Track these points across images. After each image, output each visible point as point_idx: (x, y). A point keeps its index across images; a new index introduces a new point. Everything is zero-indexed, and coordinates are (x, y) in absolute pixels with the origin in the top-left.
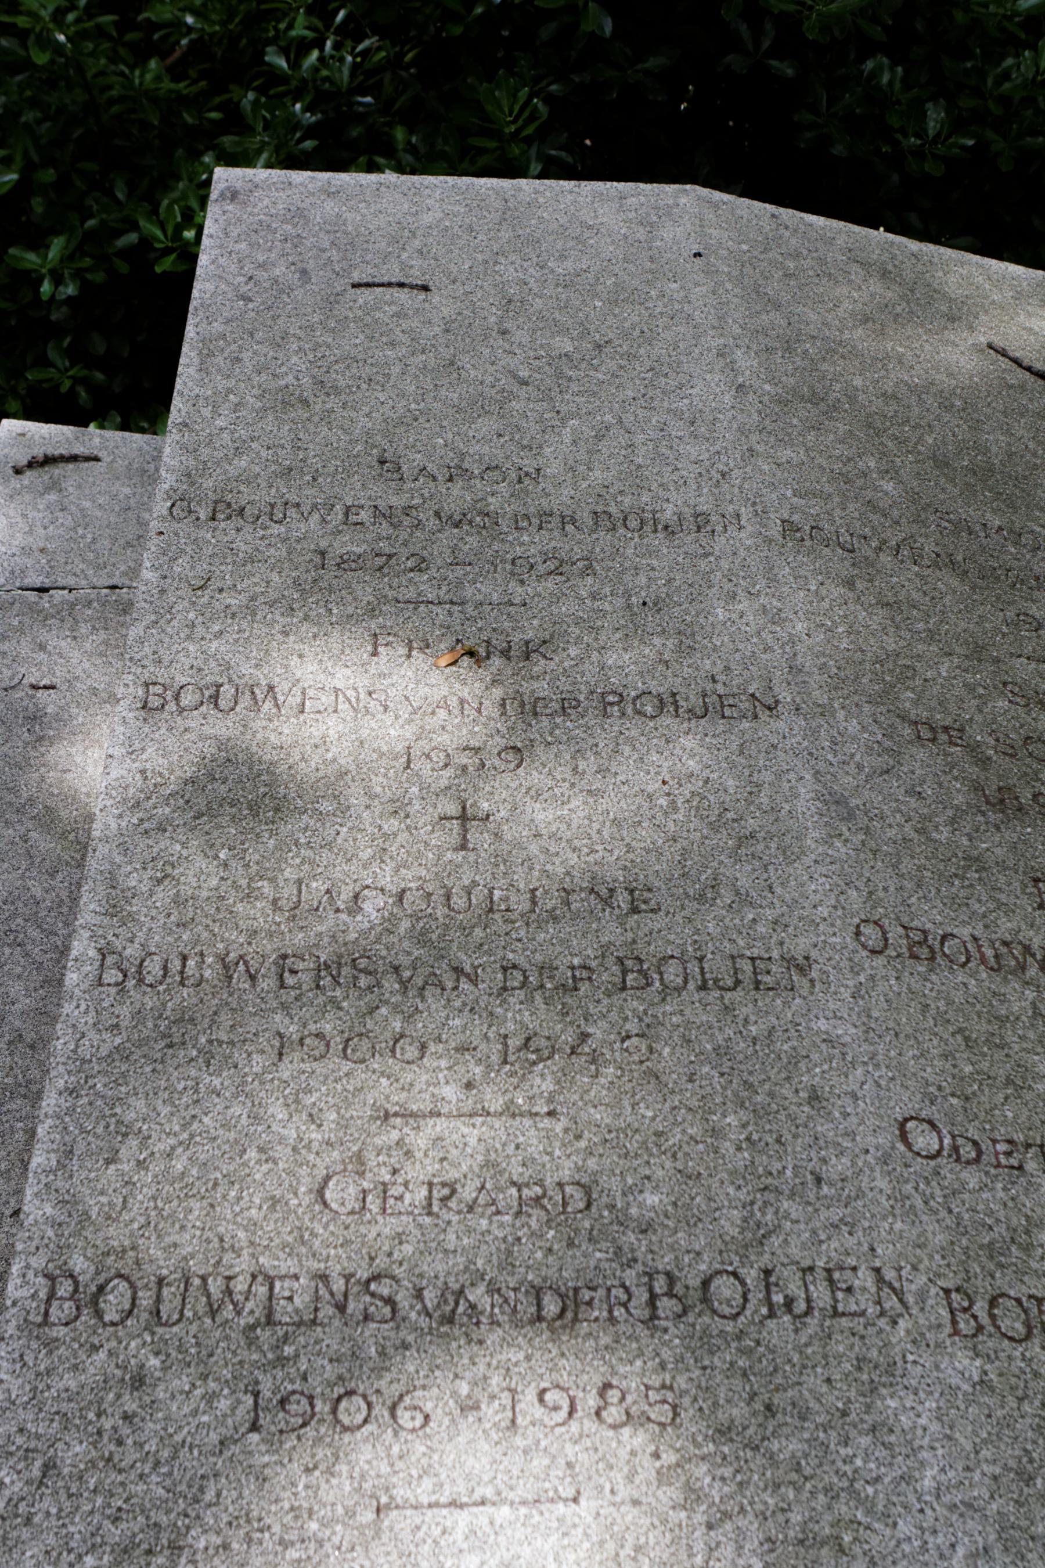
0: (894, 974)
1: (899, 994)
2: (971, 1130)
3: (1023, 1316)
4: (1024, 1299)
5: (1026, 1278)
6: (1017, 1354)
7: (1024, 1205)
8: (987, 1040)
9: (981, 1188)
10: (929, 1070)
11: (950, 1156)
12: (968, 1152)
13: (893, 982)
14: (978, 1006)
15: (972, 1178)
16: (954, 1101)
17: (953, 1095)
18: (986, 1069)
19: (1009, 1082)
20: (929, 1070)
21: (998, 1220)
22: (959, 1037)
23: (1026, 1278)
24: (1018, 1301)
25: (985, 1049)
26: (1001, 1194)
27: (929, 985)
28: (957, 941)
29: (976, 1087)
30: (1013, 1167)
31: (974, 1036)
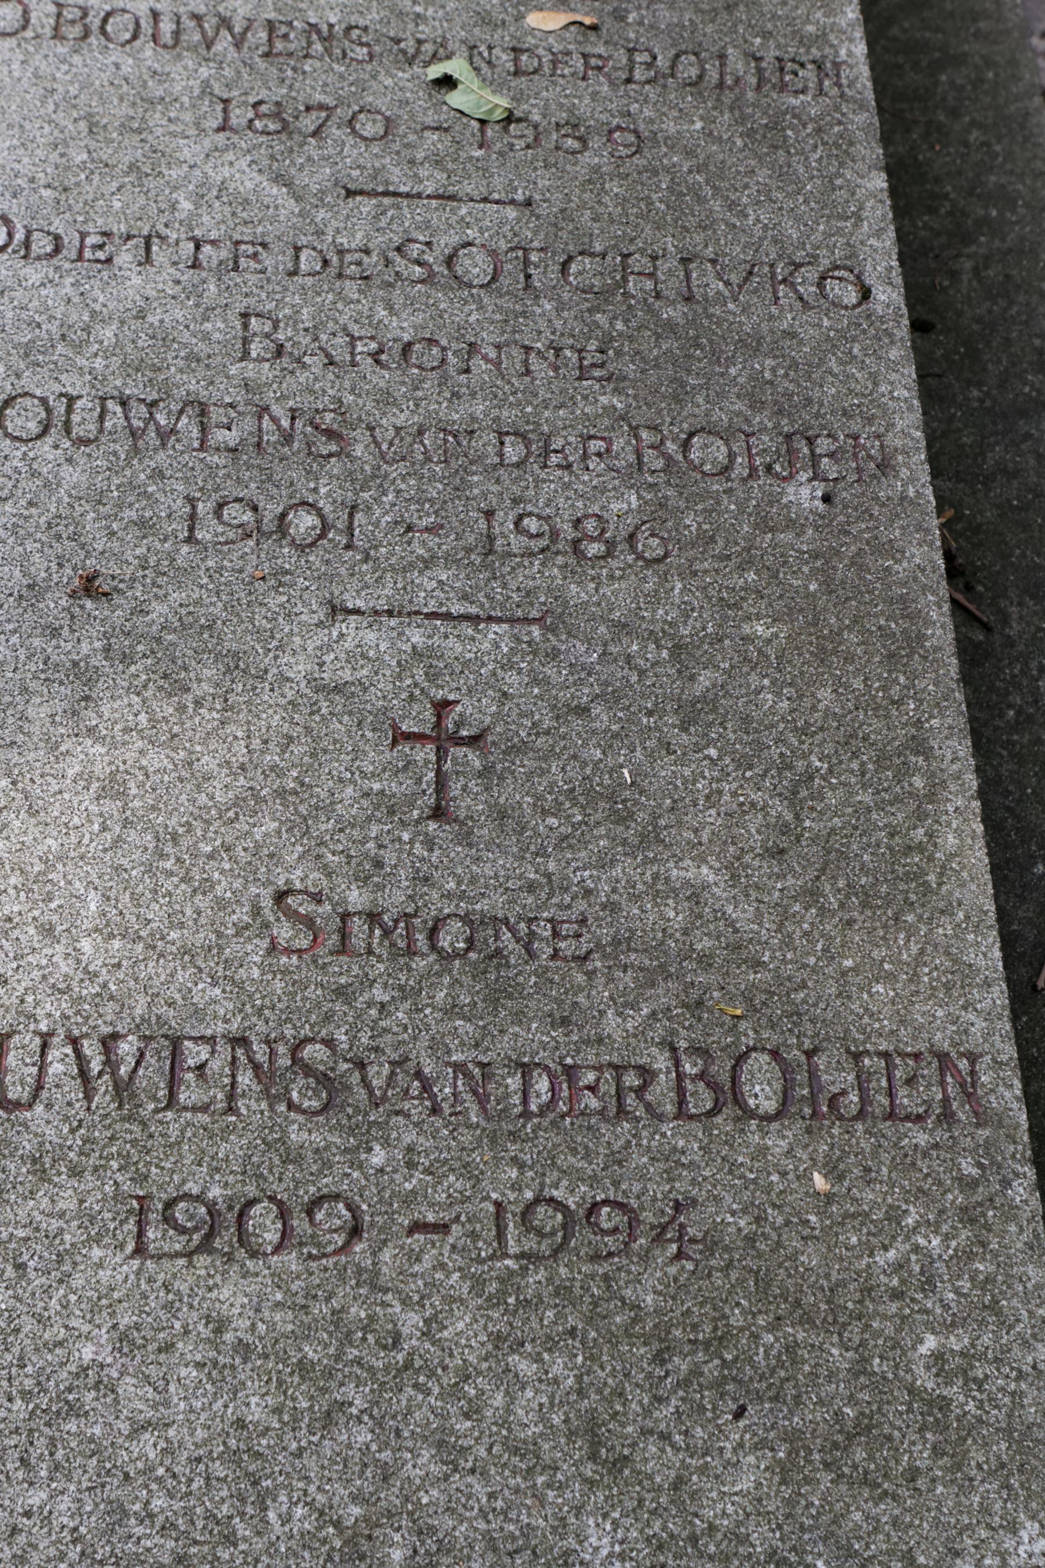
0: (21, 57)
1: (19, 80)
2: (56, 224)
3: (43, 415)
4: (52, 398)
5: (63, 377)
6: (19, 454)
7: (95, 301)
8: (123, 125)
9: (43, 284)
10: (26, 160)
11: (15, 252)
12: (42, 244)
13: (16, 66)
14: (125, 88)
15: (33, 274)
16: (46, 193)
17: (48, 186)
18: (104, 157)
19: (133, 167)
20: (26, 160)
21: (52, 318)
22: (83, 125)
23: (63, 377)
24: (44, 401)
25: (115, 135)
26: (68, 290)
27: (65, 67)
28: (127, 16)
29: (83, 176)
30: (98, 261)
31: (105, 121)
